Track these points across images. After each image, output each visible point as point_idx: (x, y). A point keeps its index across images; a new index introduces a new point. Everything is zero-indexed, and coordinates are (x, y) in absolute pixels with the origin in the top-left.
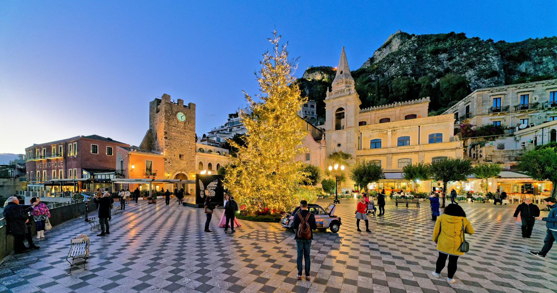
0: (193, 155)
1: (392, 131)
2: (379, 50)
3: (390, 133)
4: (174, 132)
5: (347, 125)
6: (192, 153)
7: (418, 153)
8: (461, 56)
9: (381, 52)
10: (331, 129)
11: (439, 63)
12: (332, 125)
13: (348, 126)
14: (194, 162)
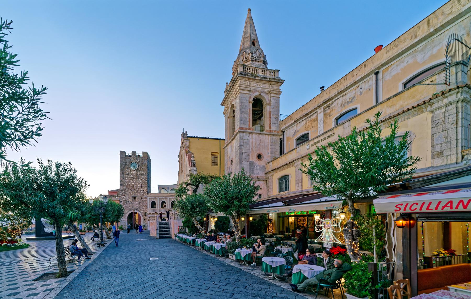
0: (145, 196)
1: (324, 109)
3: (322, 114)
4: (128, 179)
6: (144, 194)
14: (146, 202)
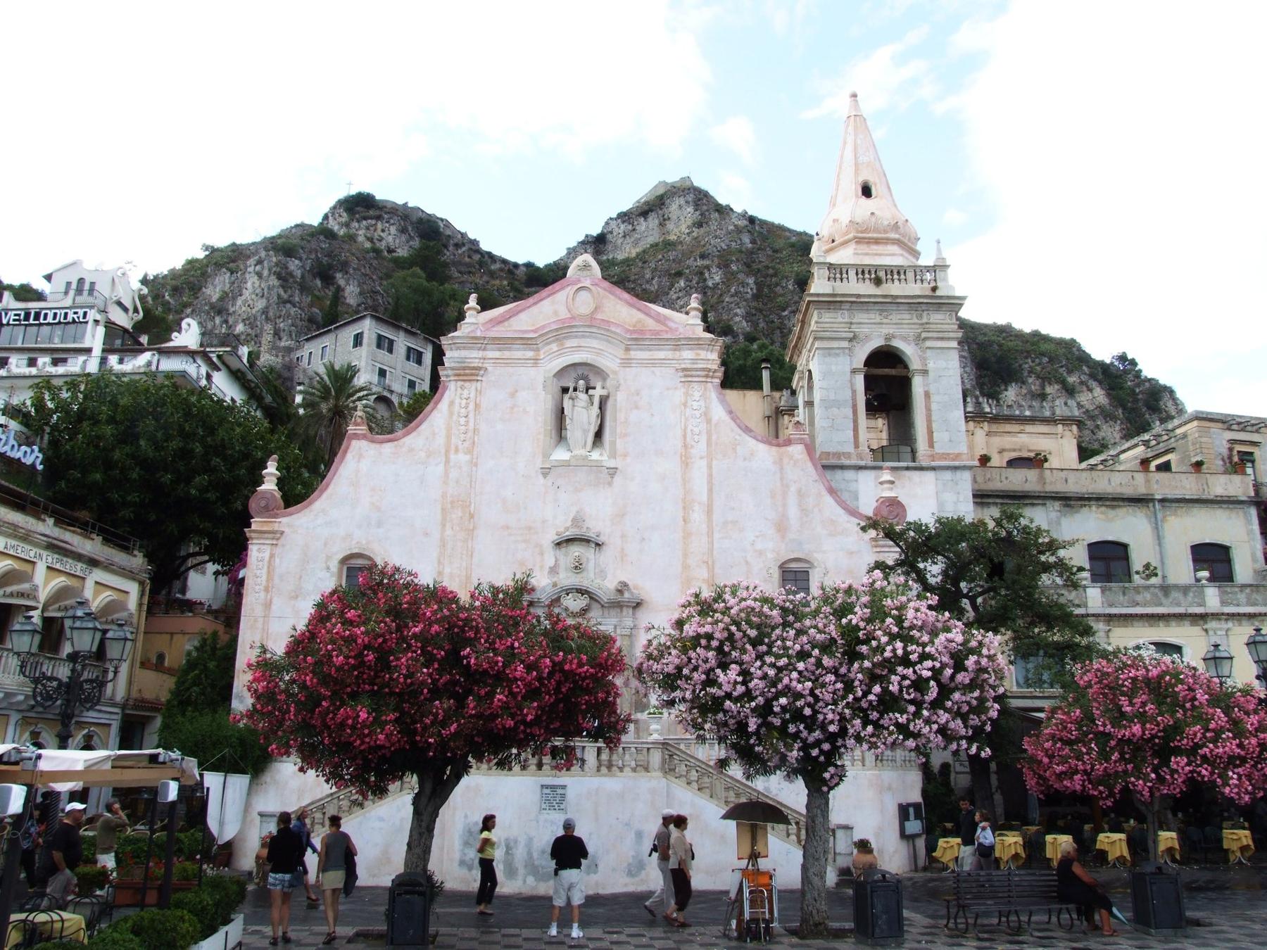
2: (625, 217)
5: (931, 444)
7: (1202, 622)
9: (630, 227)
10: (850, 448)
13: (938, 449)
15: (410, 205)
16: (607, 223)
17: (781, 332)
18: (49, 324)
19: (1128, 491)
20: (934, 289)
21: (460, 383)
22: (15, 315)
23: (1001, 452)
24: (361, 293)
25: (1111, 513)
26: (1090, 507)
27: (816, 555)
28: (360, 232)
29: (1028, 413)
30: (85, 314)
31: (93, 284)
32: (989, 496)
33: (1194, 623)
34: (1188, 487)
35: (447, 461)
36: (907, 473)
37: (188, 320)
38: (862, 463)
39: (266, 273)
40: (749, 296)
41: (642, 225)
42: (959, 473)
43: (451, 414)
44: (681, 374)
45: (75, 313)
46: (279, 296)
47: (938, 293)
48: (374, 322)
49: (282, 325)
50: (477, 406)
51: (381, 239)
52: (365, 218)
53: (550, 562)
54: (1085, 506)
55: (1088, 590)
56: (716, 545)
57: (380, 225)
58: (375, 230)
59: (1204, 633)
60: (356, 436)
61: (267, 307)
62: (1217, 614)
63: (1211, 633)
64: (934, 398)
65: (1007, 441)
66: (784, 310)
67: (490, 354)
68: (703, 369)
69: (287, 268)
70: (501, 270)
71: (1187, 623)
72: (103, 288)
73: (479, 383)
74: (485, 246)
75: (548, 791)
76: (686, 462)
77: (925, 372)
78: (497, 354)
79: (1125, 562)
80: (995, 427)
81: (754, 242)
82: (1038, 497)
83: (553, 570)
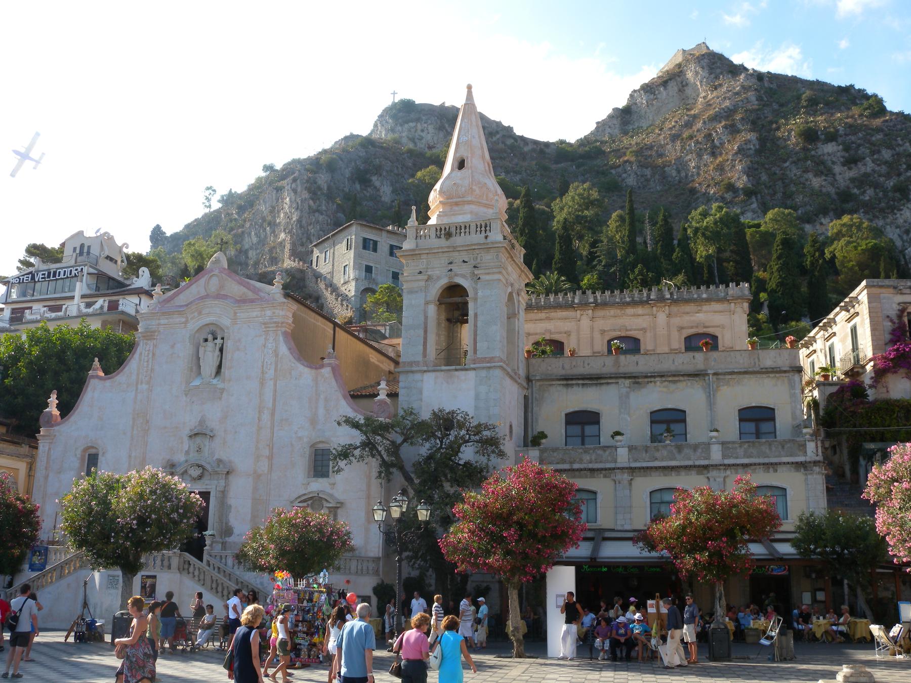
7: (705, 472)
8: (878, 160)
10: (419, 358)
11: (823, 168)
12: (425, 339)
13: (479, 355)
15: (446, 105)
16: (631, 96)
17: (783, 183)
18: (61, 279)
19: (689, 368)
20: (486, 237)
21: (145, 341)
22: (43, 274)
23: (681, 329)
24: (393, 192)
25: (673, 387)
26: (655, 382)
27: (332, 439)
28: (404, 134)
29: (704, 296)
30: (82, 269)
31: (89, 247)
32: (572, 379)
33: (699, 473)
34: (741, 361)
35: (137, 389)
36: (456, 373)
37: (143, 269)
38: (425, 368)
39: (299, 189)
40: (752, 152)
41: (663, 92)
42: (491, 371)
43: (140, 360)
44: (263, 326)
45: (76, 270)
46: (310, 207)
47: (489, 240)
48: (359, 228)
49: (312, 231)
50: (154, 354)
51: (421, 138)
52: (407, 122)
53: (186, 447)
54: (651, 382)
55: (619, 450)
56: (275, 435)
57: (419, 125)
58: (416, 130)
59: (707, 480)
60: (93, 377)
61: (301, 217)
62: (716, 465)
63: (711, 480)
64: (480, 318)
65: (686, 320)
66: (785, 161)
67: (162, 322)
68: (275, 323)
69: (316, 183)
70: (533, 150)
71: (694, 472)
72: (95, 251)
73: (155, 341)
74: (518, 132)
75: (111, 578)
76: (262, 383)
77: (475, 299)
78: (166, 321)
79: (684, 424)
80: (675, 309)
81: (759, 99)
82: (611, 378)
83: (187, 453)
